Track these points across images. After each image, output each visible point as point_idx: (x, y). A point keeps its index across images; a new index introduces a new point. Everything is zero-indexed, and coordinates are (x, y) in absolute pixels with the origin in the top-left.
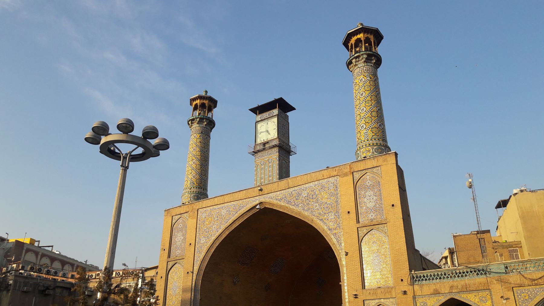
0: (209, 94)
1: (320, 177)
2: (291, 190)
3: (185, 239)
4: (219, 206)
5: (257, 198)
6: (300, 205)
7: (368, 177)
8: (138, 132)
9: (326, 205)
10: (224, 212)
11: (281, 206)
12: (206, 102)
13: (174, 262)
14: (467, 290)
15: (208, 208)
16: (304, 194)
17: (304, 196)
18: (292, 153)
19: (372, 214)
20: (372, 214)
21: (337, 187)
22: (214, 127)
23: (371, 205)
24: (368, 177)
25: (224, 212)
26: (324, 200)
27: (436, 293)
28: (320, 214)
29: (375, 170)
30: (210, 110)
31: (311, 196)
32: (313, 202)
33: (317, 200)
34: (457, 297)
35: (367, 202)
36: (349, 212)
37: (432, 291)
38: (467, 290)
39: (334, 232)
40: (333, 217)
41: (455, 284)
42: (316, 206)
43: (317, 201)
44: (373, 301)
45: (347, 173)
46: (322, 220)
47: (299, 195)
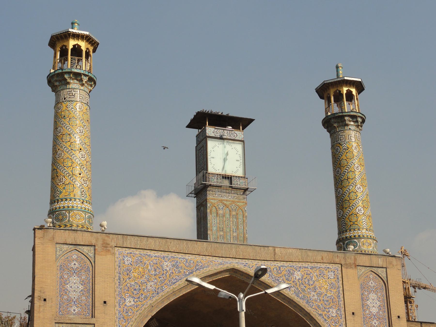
1: (319, 258)
2: (279, 264)
9: (325, 298)
10: (167, 265)
15: (137, 252)
16: (298, 275)
17: (297, 278)
19: (375, 321)
20: (375, 321)
21: (338, 278)
25: (167, 265)
26: (323, 290)
28: (318, 306)
31: (306, 280)
32: (309, 289)
33: (315, 289)
35: (371, 305)
36: (353, 313)
40: (334, 315)
43: (315, 289)
45: (350, 264)
46: (320, 315)
47: (290, 273)
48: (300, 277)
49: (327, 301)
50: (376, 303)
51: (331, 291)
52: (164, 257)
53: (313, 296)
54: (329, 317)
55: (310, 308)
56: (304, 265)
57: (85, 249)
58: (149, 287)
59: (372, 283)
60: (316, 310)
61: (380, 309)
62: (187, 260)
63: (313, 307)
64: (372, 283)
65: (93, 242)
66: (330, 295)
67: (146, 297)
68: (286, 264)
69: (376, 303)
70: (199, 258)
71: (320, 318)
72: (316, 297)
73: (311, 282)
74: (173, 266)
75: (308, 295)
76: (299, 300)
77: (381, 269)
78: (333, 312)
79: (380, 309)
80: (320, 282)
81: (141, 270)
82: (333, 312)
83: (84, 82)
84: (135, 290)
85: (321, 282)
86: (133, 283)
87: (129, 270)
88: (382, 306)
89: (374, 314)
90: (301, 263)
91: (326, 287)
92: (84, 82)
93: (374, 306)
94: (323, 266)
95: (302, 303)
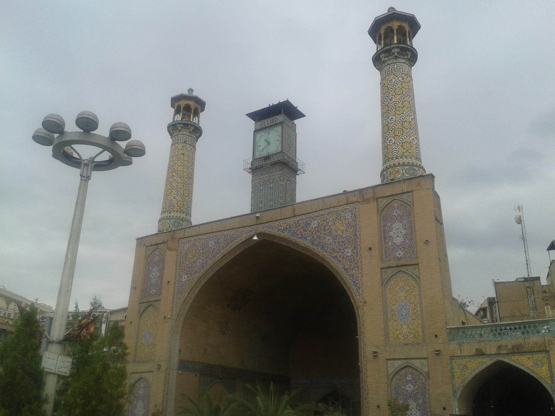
0: (195, 94)
2: (298, 218)
3: (161, 277)
4: (206, 236)
5: (254, 227)
6: (309, 238)
7: (396, 205)
8: (103, 131)
9: (341, 240)
11: (284, 239)
12: (192, 104)
13: (147, 304)
14: (518, 350)
15: (192, 239)
16: (314, 224)
18: (299, 172)
19: (399, 252)
20: (399, 252)
21: (355, 217)
22: (200, 135)
23: (398, 240)
24: (396, 205)
25: (211, 243)
26: (340, 232)
27: (480, 353)
28: (333, 249)
29: (404, 196)
30: (196, 114)
31: (323, 227)
32: (325, 234)
33: (330, 233)
34: (506, 360)
36: (370, 249)
37: (473, 351)
38: (518, 350)
39: (352, 272)
40: (350, 255)
41: (504, 343)
42: (329, 240)
44: (399, 361)
47: (307, 224)
48: (316, 225)
49: (343, 242)
50: (401, 232)
51: (347, 231)
52: (210, 238)
53: (329, 240)
54: (343, 258)
55: (325, 253)
56: (321, 212)
57: (162, 246)
58: (198, 264)
59: (396, 212)
60: (331, 253)
61: (406, 237)
62: (225, 235)
63: (328, 251)
64: (396, 212)
65: (166, 240)
66: (346, 235)
67: (195, 272)
68: (304, 217)
69: (401, 232)
70: (233, 232)
71: (334, 260)
72: (331, 241)
73: (327, 228)
74: (215, 242)
75: (323, 241)
76: (314, 247)
77: (406, 195)
78: (348, 252)
79: (406, 237)
80: (337, 225)
81: (194, 251)
82: (349, 252)
83: (179, 129)
84: (189, 268)
85: (337, 225)
86: (188, 263)
87: (187, 254)
88: (408, 233)
89: (399, 244)
90: (317, 212)
91: (341, 228)
92: (179, 129)
93: (398, 236)
94: (340, 209)
95: (317, 249)
